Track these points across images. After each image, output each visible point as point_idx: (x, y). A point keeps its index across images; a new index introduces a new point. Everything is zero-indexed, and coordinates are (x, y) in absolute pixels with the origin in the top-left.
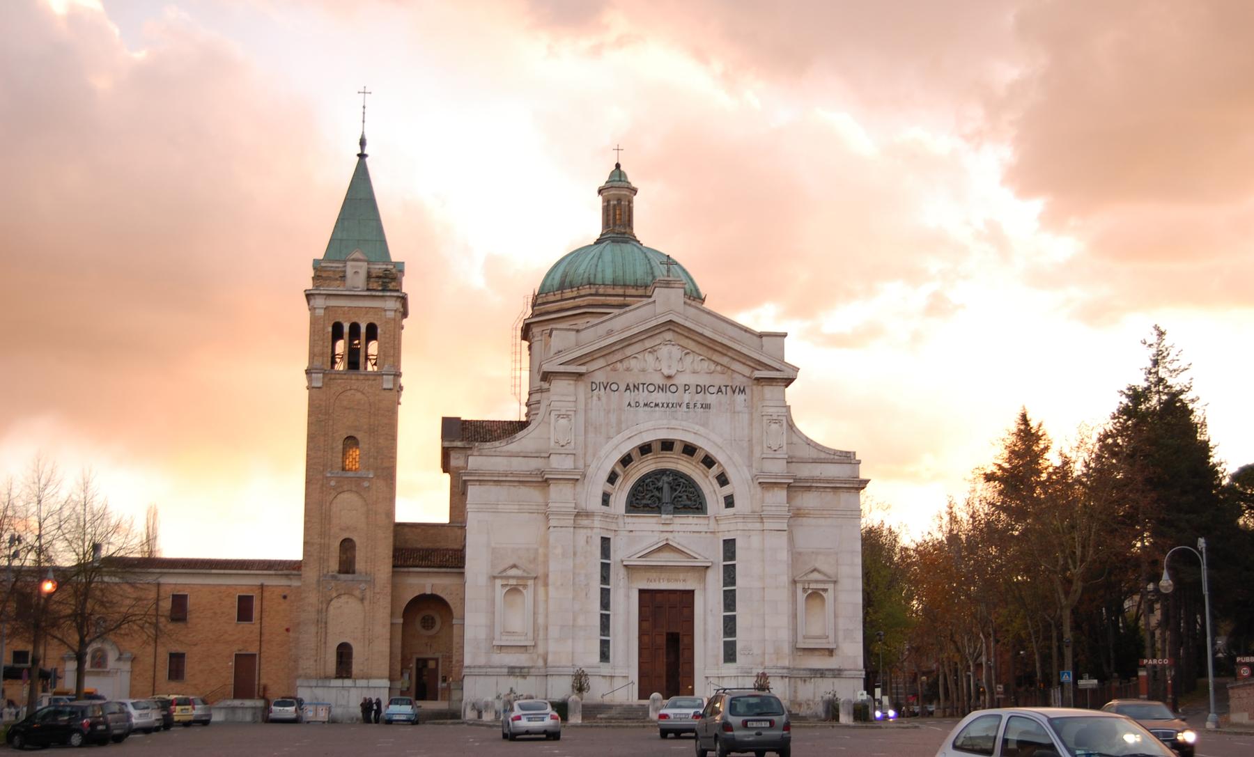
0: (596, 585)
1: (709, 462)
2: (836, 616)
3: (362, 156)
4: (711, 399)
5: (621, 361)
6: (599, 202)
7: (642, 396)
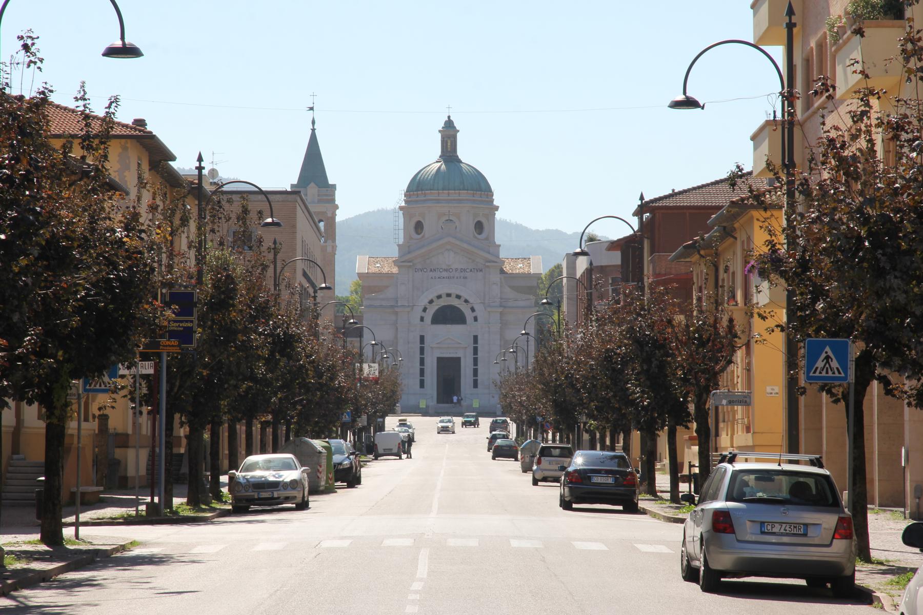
0: (418, 356)
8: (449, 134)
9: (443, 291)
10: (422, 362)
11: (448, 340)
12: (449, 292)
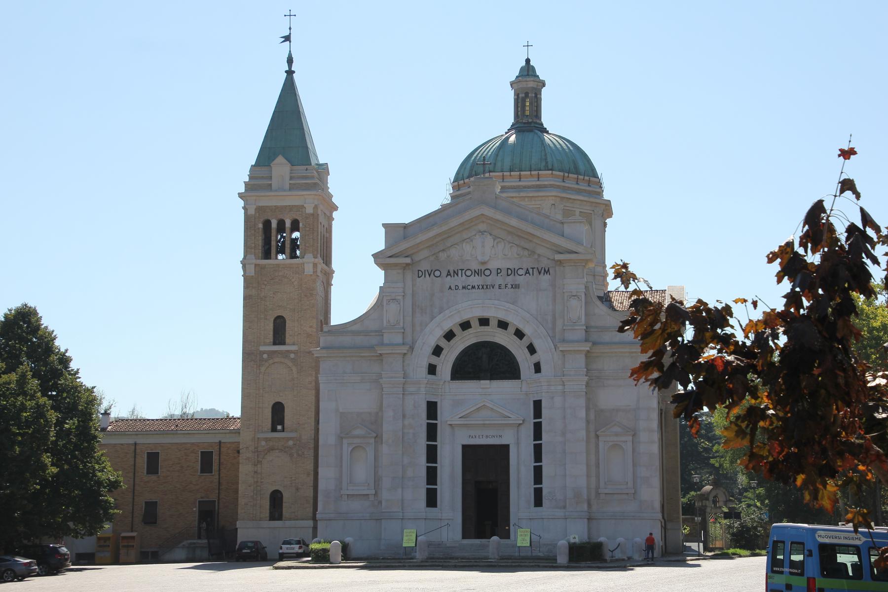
0: (422, 442)
1: (519, 334)
2: (634, 465)
3: (290, 73)
4: (520, 280)
5: (443, 250)
6: (510, 95)
7: (460, 280)
8: (528, 91)
9: (472, 313)
10: (432, 454)
11: (483, 411)
12: (485, 314)
